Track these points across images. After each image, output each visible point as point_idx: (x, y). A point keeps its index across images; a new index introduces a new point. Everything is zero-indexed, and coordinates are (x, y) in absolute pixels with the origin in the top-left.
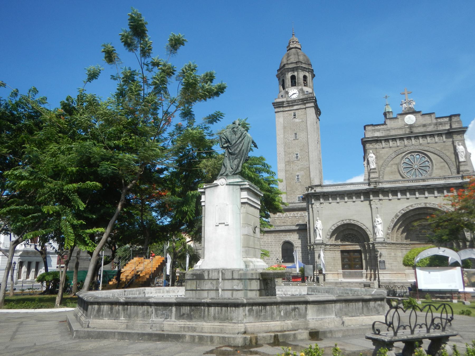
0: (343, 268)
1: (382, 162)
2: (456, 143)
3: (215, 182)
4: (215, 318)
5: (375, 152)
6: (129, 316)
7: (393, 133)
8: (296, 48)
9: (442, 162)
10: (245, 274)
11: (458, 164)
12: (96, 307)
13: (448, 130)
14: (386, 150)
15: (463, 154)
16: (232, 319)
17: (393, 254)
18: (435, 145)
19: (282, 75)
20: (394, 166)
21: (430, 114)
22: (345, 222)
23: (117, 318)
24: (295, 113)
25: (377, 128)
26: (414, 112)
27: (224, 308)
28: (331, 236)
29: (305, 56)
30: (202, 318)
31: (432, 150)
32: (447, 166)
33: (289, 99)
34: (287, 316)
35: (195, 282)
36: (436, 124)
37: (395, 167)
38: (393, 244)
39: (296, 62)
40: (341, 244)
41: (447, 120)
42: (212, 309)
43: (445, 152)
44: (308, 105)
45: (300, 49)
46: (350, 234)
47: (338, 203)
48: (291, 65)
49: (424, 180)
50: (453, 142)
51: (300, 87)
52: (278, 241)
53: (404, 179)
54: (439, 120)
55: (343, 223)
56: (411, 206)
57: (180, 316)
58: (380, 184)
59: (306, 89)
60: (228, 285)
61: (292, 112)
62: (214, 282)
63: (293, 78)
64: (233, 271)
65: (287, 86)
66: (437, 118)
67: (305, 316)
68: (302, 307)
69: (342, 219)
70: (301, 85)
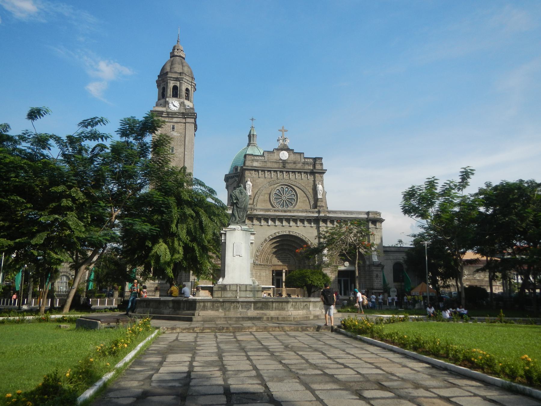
1: (257, 190)
2: (317, 182)
3: (230, 227)
4: (276, 309)
5: (252, 180)
6: (224, 309)
7: (269, 165)
8: (180, 56)
9: (304, 197)
10: (254, 288)
11: (316, 200)
12: (202, 304)
13: (312, 170)
14: (263, 180)
15: (321, 193)
16: (285, 309)
17: (258, 274)
18: (301, 182)
19: (164, 82)
20: (266, 195)
21: (300, 154)
23: (218, 310)
24: (173, 126)
25: (255, 158)
26: (288, 150)
27: (281, 304)
29: (189, 67)
30: (267, 309)
31: (298, 186)
32: (308, 201)
33: (169, 110)
34: (303, 308)
35: (220, 292)
36: (304, 163)
37: (267, 196)
38: (260, 265)
39: (180, 73)
41: (311, 160)
42: (274, 304)
43: (308, 188)
44: (188, 120)
45: (184, 58)
48: (174, 74)
49: (290, 211)
50: (314, 181)
51: (182, 100)
53: (274, 209)
54: (306, 160)
56: (278, 233)
57: (255, 309)
58: (255, 211)
59: (187, 103)
60: (243, 294)
61: (172, 124)
62: (234, 292)
63: (175, 88)
64: (246, 286)
65: (168, 95)
66: (305, 158)
67: (309, 308)
68: (308, 304)
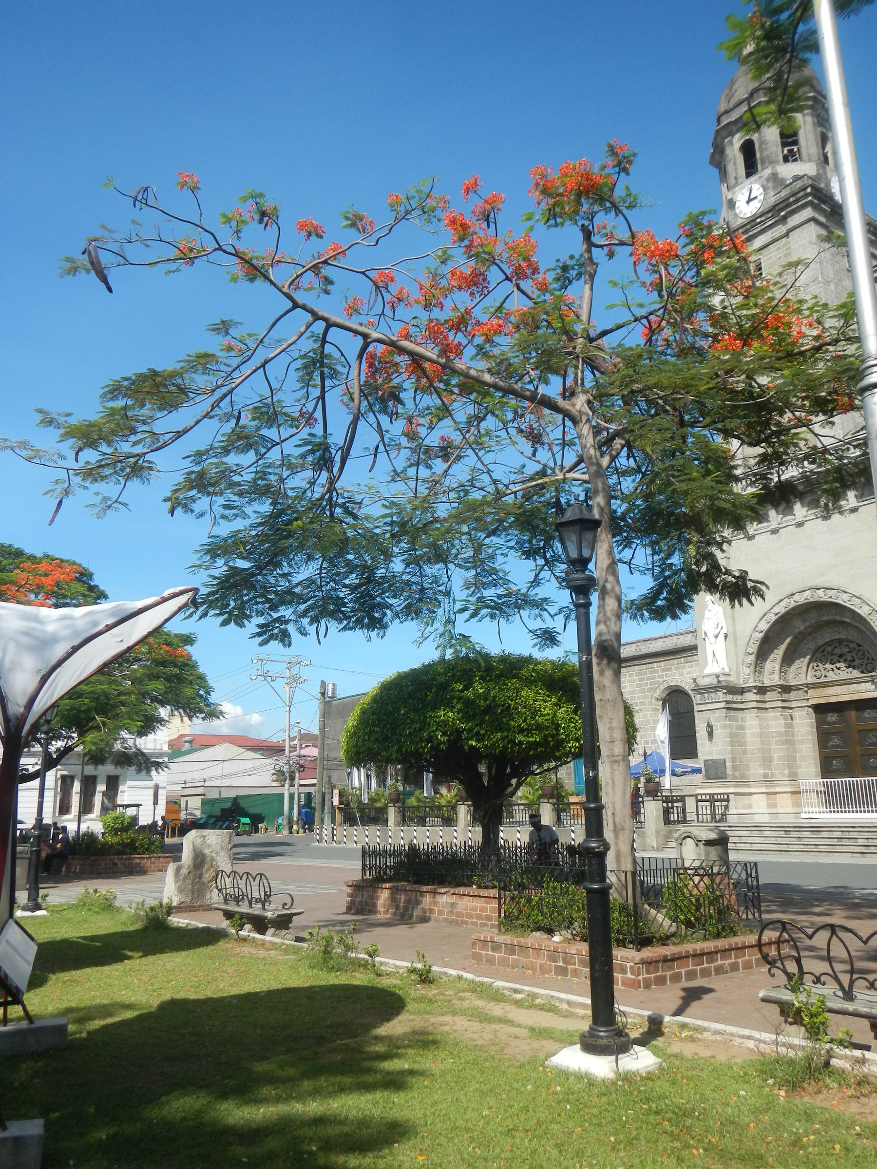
0: (827, 771)
22: (800, 599)
28: (763, 653)
40: (810, 679)
46: (840, 641)
47: (774, 532)
51: (768, 172)
52: (649, 690)
55: (793, 604)
63: (748, 150)
69: (789, 593)
70: (773, 162)
